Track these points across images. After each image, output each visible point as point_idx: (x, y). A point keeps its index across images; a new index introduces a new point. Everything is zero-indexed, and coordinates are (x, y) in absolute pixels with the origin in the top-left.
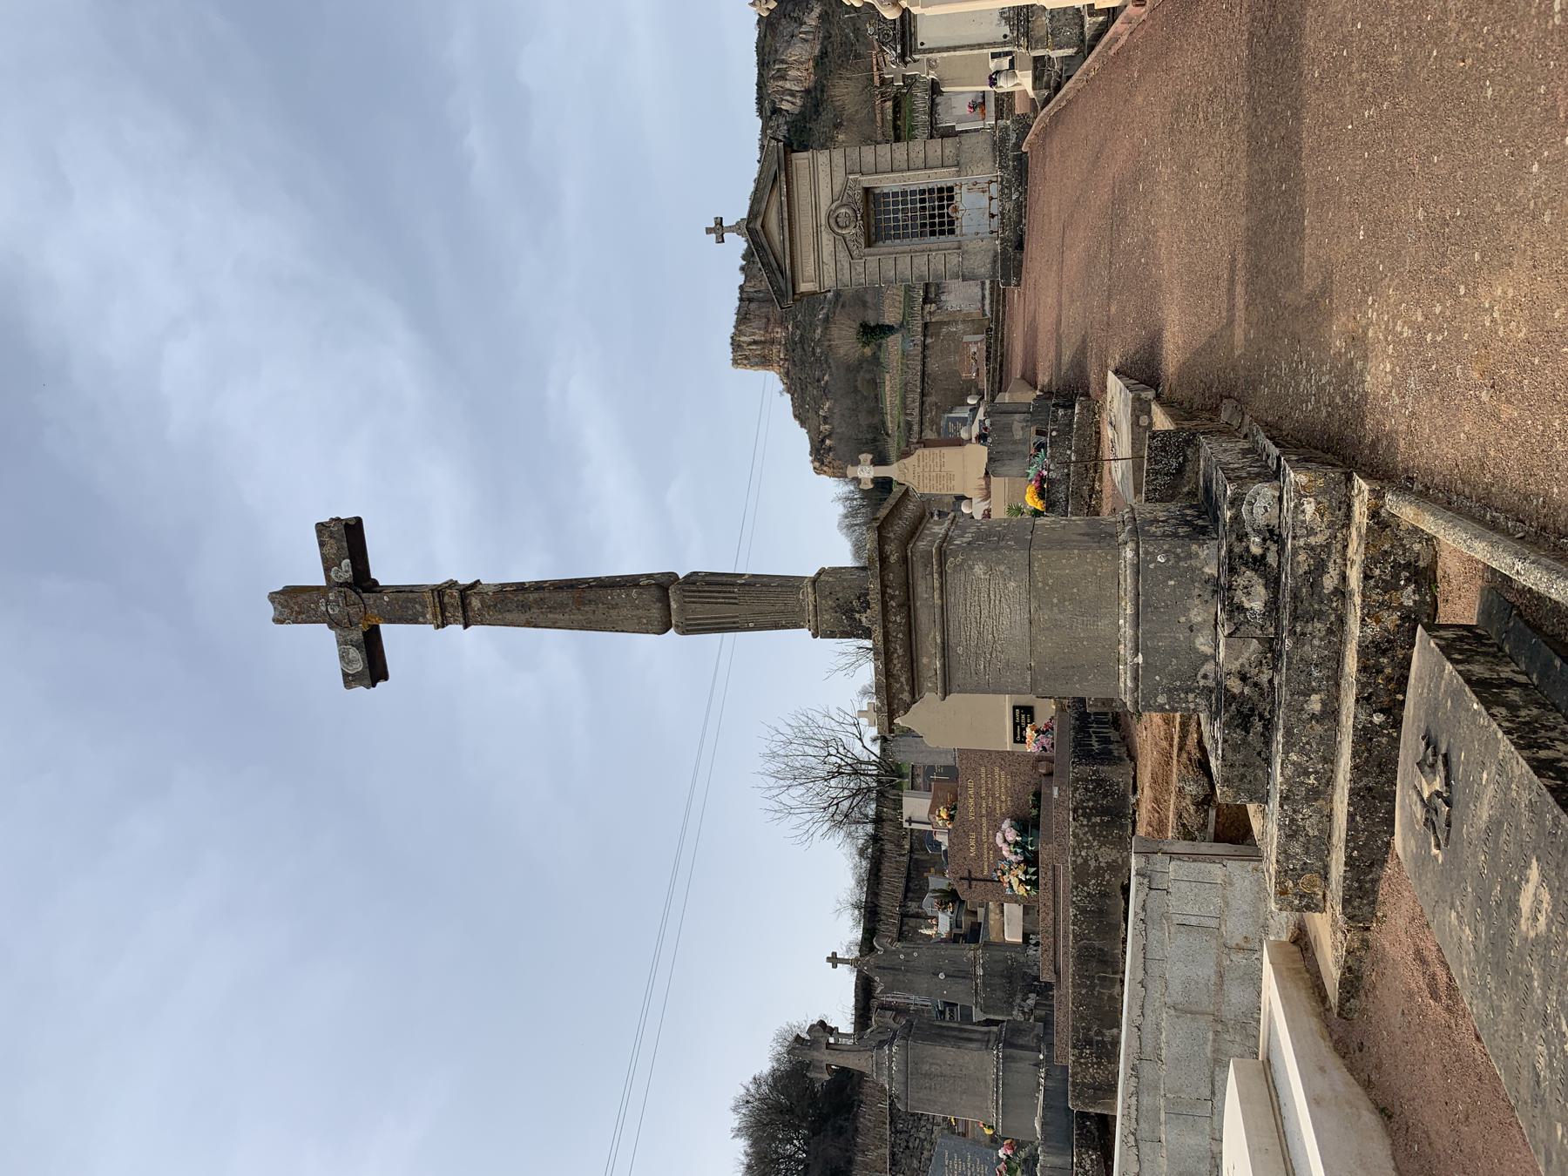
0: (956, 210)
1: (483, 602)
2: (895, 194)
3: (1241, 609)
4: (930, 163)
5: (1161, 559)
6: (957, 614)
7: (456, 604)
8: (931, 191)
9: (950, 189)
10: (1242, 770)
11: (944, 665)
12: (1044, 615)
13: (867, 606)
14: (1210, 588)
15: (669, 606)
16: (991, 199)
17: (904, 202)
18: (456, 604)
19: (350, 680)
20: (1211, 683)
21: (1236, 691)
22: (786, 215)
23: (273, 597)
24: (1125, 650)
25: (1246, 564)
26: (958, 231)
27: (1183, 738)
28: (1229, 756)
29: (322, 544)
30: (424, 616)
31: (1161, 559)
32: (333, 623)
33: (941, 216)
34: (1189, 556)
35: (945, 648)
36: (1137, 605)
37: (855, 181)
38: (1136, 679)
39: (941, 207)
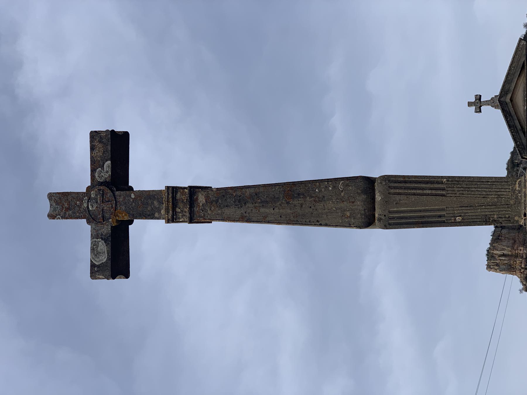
1: (207, 198)
7: (186, 204)
15: (373, 199)
18: (186, 204)
19: (96, 271)
23: (51, 196)
29: (92, 148)
30: (159, 212)
32: (91, 219)
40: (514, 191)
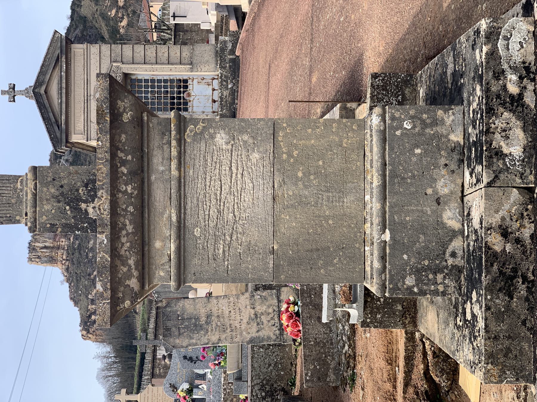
0: (189, 95)
2: (146, 81)
3: (499, 154)
4: (171, 61)
5: (407, 125)
6: (196, 189)
8: (172, 81)
9: (186, 81)
10: (507, 343)
11: (179, 250)
12: (289, 191)
13: (93, 197)
14: (456, 157)
16: (214, 90)
17: (153, 87)
20: (459, 262)
21: (498, 248)
22: (64, 85)
24: (371, 229)
25: (503, 104)
26: (190, 110)
27: (408, 373)
28: (493, 326)
31: (407, 125)
33: (179, 98)
34: (435, 122)
35: (181, 229)
36: (384, 176)
37: (117, 67)
38: (383, 258)
39: (180, 92)
40: (15, 189)
